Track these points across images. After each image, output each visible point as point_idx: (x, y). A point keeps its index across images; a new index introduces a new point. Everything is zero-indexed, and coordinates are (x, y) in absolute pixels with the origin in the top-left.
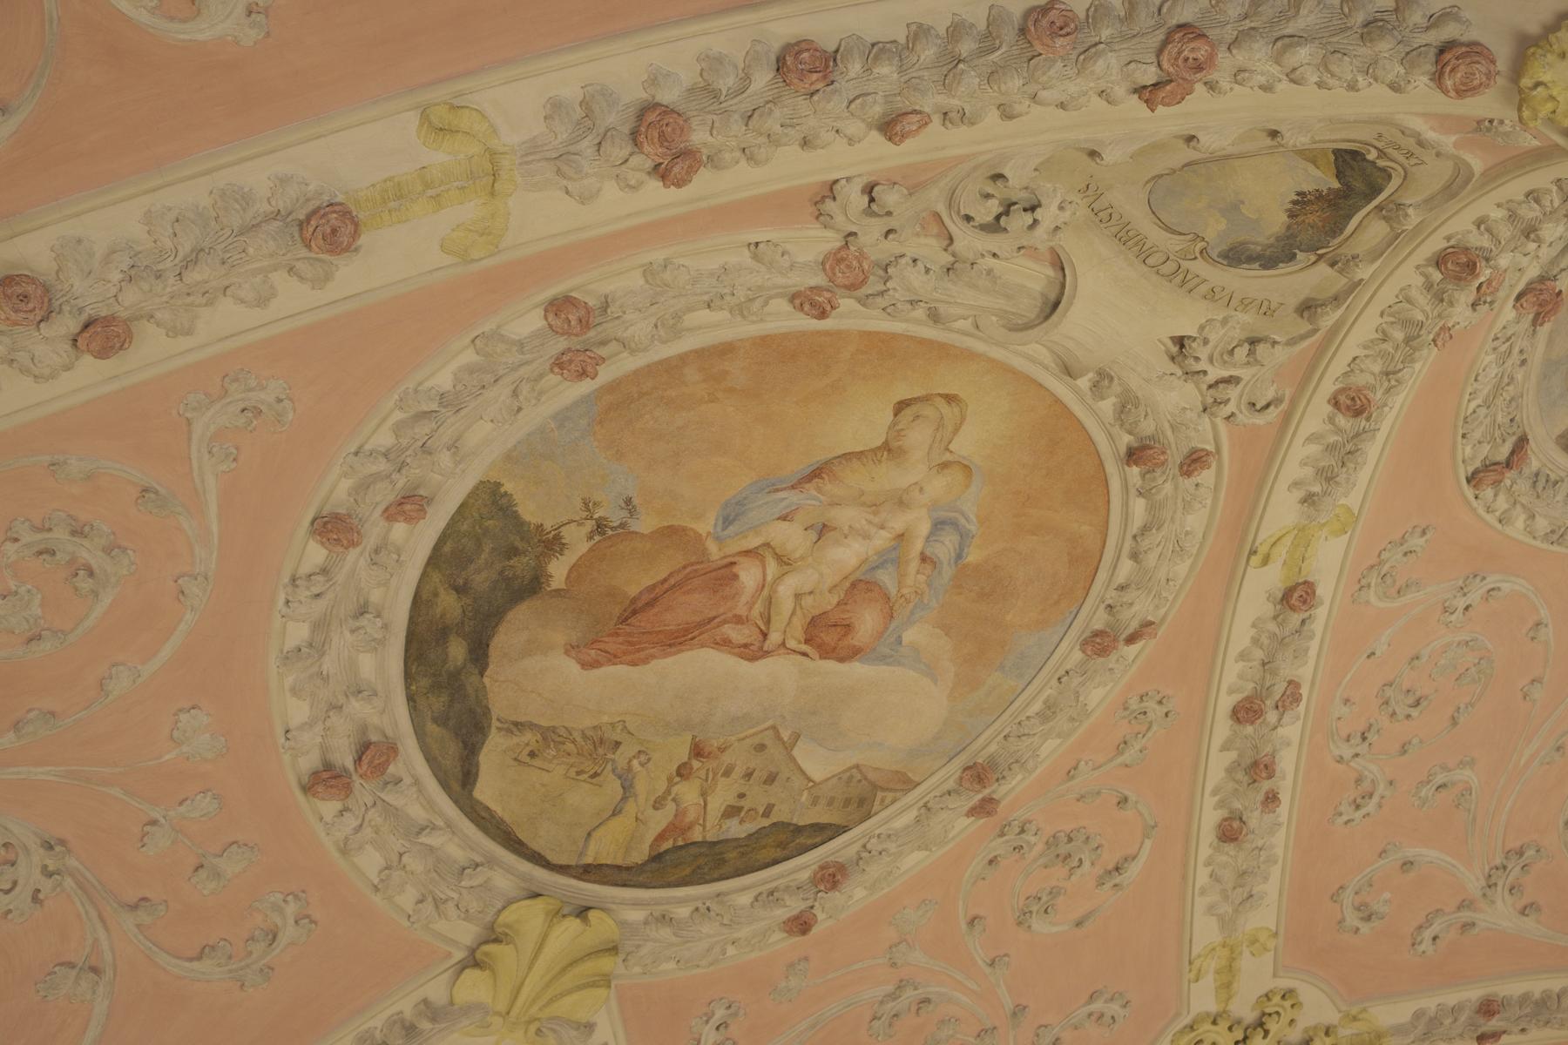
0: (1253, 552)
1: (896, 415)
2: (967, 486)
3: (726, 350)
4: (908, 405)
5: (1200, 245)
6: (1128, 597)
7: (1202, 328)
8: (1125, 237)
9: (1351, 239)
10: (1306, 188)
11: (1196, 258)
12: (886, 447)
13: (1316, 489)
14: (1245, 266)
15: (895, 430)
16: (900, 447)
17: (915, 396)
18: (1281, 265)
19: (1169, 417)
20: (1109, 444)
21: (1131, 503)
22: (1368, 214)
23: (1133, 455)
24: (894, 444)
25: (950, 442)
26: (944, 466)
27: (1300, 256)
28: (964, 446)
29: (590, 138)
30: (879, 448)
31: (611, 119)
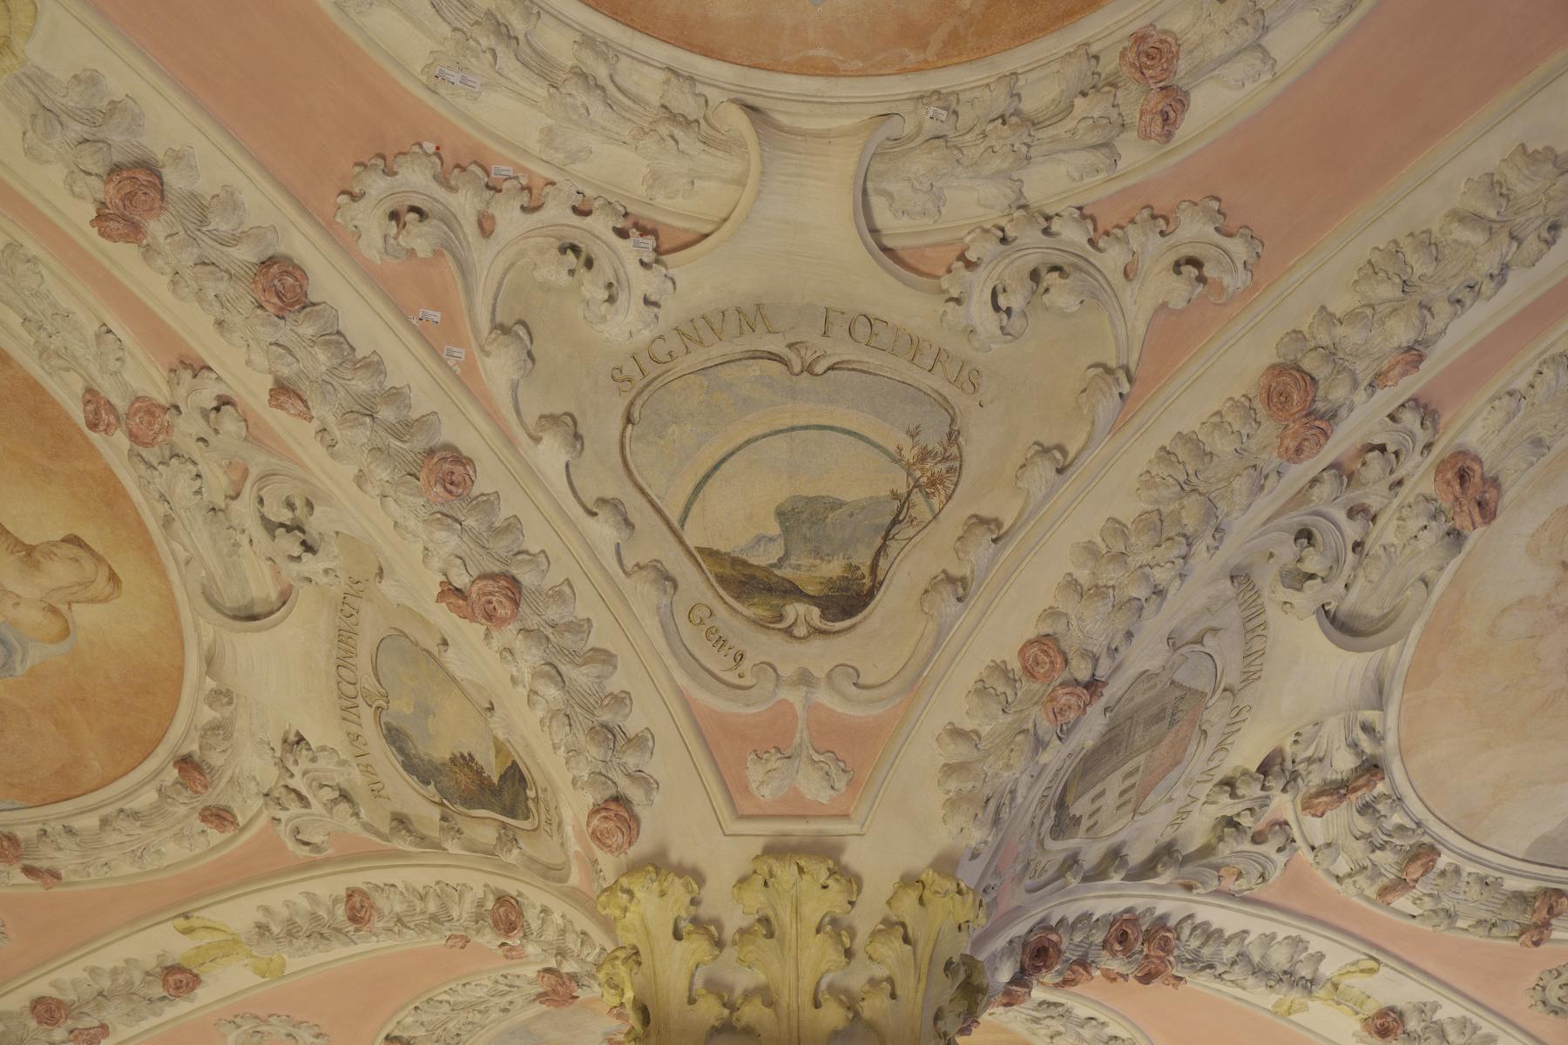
0: (186, 916)
1: (63, 540)
2: (51, 642)
4: (80, 546)
5: (382, 703)
6: (64, 841)
7: (323, 749)
8: (345, 637)
9: (469, 819)
10: (477, 757)
11: (371, 706)
12: (30, 550)
13: (276, 929)
14: (394, 750)
15: (50, 549)
16: (39, 562)
17: (93, 547)
18: (415, 778)
19: (237, 771)
20: (181, 735)
21: (146, 788)
22: (495, 819)
23: (186, 763)
24: (37, 555)
25: (78, 602)
26: (54, 610)
27: (431, 787)
28: (85, 616)
29: (86, 128)
30: (24, 544)
31: (116, 138)
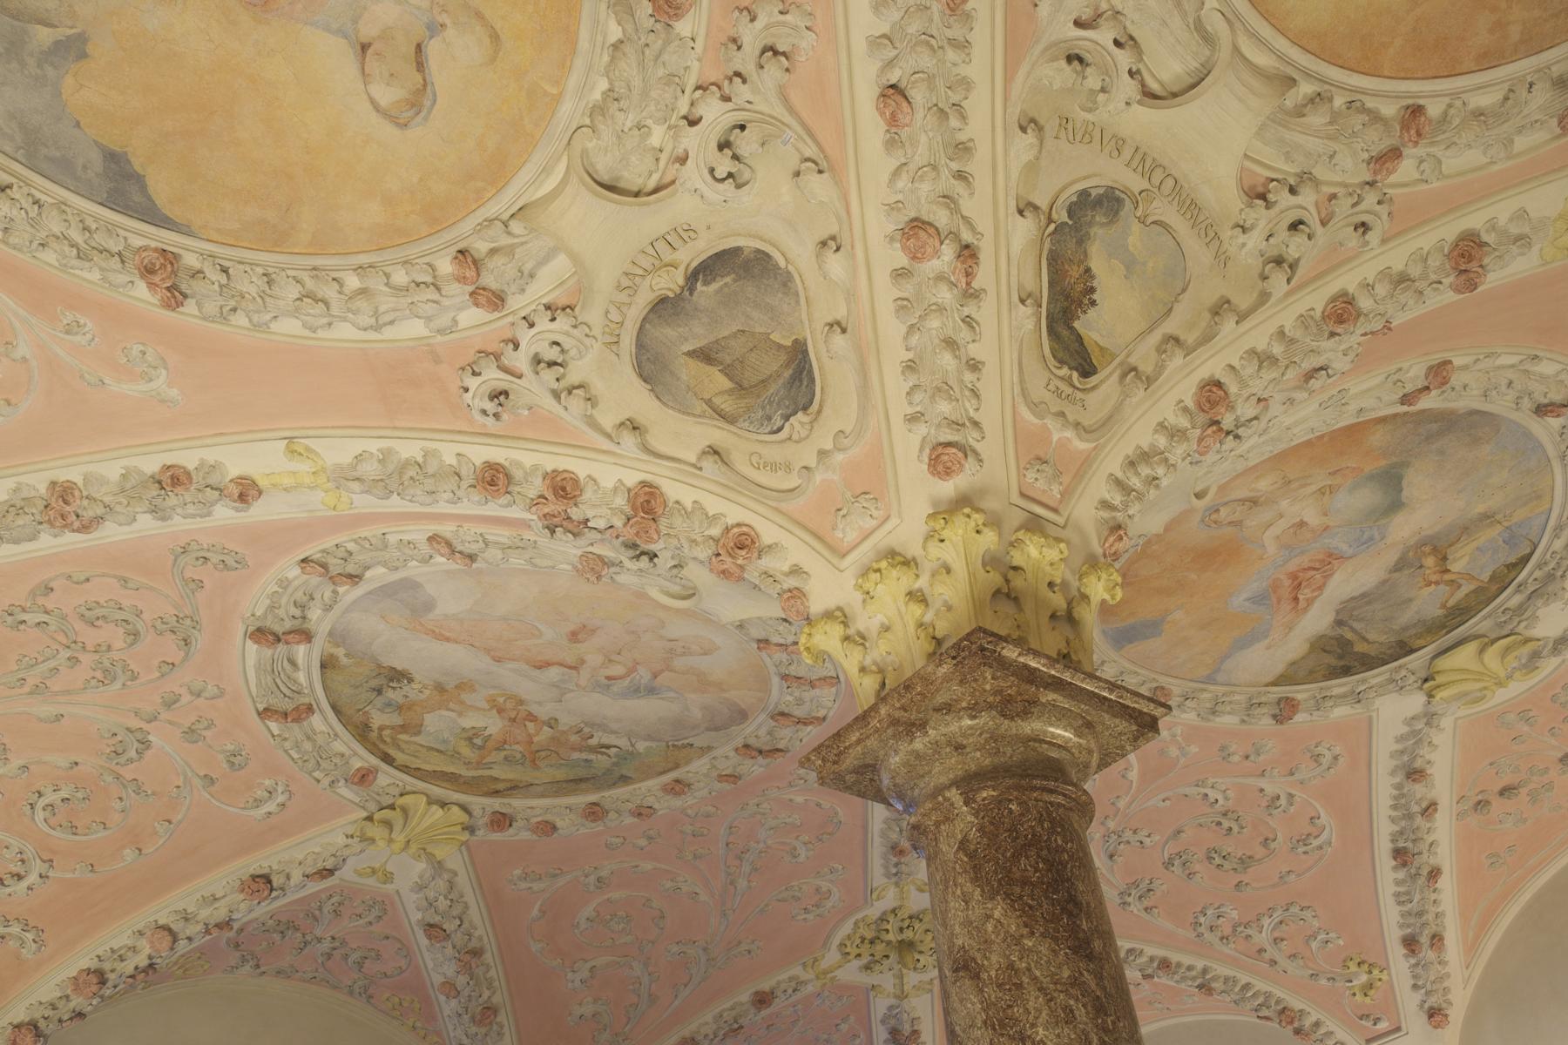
3: (1489, 59)
8: (1191, 207)
10: (1092, 313)
14: (1101, 191)
18: (1074, 199)
27: (1064, 217)
